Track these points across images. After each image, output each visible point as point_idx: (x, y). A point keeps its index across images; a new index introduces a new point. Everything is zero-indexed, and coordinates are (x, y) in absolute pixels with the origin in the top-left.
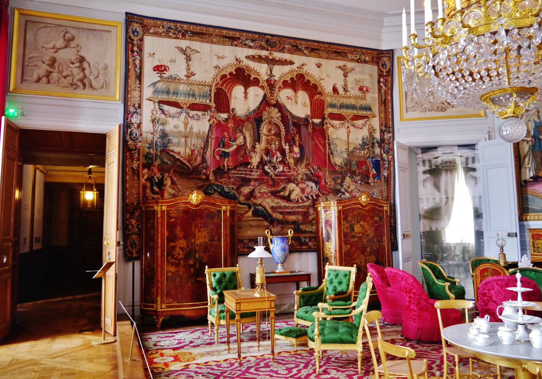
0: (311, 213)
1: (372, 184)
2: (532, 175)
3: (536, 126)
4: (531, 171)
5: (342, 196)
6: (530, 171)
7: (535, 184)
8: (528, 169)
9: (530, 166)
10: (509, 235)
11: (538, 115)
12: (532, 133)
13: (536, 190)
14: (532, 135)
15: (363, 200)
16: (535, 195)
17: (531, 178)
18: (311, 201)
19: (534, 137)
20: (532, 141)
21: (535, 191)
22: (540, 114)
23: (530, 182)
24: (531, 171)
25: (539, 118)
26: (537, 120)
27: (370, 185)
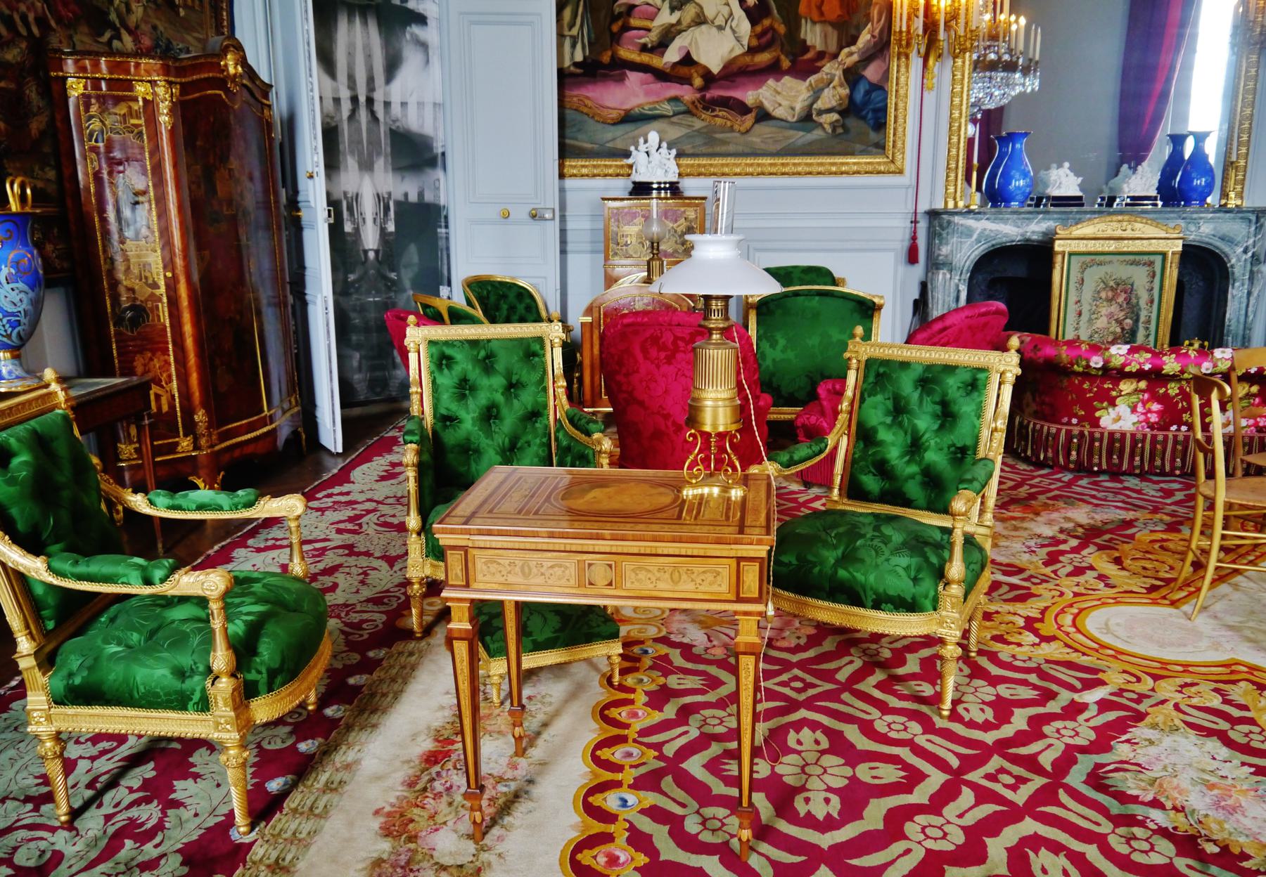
0: (35, 110)
1: (182, 12)
2: (579, 57)
4: (579, 46)
5: (116, 43)
6: (573, 46)
7: (589, 82)
8: (568, 39)
10: (534, 217)
13: (588, 98)
15: (232, 70)
16: (585, 110)
17: (576, 64)
18: (24, 45)
21: (587, 102)
23: (573, 75)
24: (579, 46)
27: (178, 13)
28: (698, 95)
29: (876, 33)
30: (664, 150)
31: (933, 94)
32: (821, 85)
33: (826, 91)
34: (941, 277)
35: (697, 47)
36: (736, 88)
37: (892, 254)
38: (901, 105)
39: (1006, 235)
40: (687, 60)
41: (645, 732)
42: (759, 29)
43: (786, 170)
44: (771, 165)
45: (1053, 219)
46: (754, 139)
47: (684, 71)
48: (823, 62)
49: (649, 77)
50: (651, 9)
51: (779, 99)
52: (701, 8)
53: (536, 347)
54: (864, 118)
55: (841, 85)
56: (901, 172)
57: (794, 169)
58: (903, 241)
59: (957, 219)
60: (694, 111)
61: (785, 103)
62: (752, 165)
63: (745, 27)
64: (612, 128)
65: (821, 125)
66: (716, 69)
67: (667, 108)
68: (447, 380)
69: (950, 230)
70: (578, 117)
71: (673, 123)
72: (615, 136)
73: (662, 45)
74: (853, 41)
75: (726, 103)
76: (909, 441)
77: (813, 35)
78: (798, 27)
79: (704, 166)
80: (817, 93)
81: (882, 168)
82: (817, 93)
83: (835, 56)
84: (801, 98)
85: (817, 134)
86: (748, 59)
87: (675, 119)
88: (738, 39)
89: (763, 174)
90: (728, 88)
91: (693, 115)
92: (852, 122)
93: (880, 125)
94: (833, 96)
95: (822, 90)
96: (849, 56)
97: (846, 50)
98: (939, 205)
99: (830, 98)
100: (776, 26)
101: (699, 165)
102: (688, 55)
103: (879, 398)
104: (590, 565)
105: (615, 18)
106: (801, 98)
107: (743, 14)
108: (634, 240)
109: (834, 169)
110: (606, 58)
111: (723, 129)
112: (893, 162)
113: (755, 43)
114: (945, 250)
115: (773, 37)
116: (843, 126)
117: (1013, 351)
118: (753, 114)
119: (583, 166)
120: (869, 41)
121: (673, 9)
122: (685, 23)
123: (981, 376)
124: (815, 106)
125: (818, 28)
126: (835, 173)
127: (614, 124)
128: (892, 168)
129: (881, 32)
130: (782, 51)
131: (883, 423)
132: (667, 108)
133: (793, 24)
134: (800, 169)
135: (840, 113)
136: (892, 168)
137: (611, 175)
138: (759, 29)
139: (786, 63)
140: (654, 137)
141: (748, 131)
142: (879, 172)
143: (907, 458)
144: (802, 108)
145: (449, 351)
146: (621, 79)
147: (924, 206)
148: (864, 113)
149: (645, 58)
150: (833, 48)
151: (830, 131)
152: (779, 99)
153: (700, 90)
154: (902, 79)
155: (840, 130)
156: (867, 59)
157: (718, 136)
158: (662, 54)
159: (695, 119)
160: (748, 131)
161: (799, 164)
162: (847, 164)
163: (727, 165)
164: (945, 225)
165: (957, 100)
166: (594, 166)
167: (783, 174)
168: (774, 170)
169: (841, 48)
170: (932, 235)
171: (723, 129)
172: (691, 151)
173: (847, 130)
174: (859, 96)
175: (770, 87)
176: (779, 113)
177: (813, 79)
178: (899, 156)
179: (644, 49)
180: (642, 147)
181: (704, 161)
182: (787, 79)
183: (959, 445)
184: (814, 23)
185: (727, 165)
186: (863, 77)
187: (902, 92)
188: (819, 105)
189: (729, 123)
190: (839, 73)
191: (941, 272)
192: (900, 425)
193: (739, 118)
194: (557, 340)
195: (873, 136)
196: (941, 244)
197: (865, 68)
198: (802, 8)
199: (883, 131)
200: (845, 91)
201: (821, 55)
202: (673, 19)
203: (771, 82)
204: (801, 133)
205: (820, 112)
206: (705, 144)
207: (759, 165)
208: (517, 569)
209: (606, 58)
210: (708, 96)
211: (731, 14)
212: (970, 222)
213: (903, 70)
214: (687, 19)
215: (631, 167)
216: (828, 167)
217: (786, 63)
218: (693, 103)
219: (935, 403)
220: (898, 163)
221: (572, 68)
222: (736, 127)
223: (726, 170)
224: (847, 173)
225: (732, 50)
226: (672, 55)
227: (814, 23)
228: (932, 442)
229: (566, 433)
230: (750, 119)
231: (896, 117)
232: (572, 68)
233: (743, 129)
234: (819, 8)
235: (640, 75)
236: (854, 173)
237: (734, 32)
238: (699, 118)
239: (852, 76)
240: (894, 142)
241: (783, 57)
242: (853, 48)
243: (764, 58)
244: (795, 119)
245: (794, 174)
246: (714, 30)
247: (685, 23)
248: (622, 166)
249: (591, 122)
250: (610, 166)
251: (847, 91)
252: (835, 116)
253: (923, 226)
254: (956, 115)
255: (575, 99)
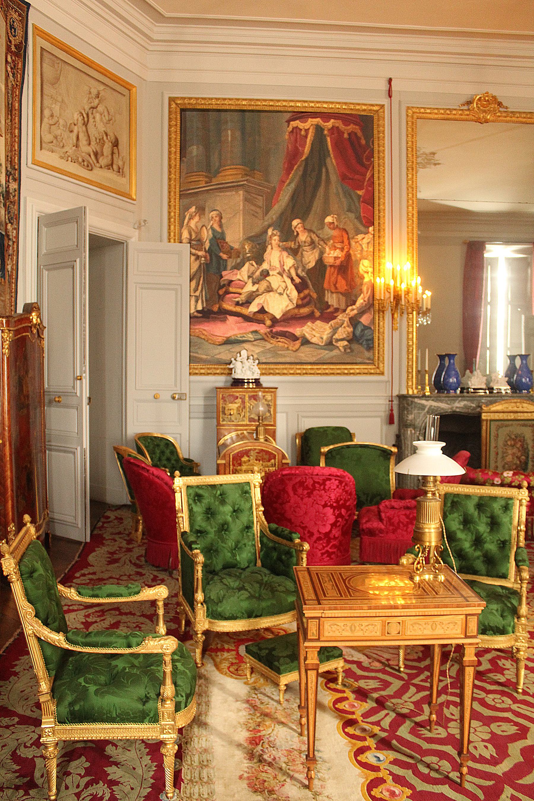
2: (200, 308)
3: (214, 236)
4: (200, 302)
6: (197, 301)
7: (204, 321)
9: (197, 294)
10: (174, 398)
11: (220, 221)
12: (207, 245)
13: (205, 330)
14: (207, 249)
16: (203, 337)
17: (198, 312)
19: (209, 251)
20: (205, 257)
21: (204, 332)
22: (223, 221)
24: (200, 302)
25: (221, 226)
26: (216, 227)
28: (268, 330)
29: (366, 299)
30: (251, 361)
31: (398, 332)
32: (337, 326)
33: (340, 329)
34: (409, 432)
35: (268, 304)
36: (290, 326)
37: (379, 420)
38: (381, 337)
39: (443, 409)
40: (262, 311)
41: (366, 715)
42: (302, 295)
43: (319, 372)
44: (311, 369)
45: (467, 400)
46: (300, 354)
47: (260, 316)
48: (338, 314)
49: (240, 319)
50: (241, 283)
51: (314, 333)
52: (270, 283)
53: (247, 488)
54: (361, 344)
55: (348, 326)
56: (382, 374)
57: (324, 372)
58: (385, 411)
59: (416, 400)
60: (266, 338)
61: (317, 335)
62: (300, 369)
63: (294, 294)
64: (219, 347)
65: (338, 347)
66: (278, 316)
67: (251, 337)
68: (198, 509)
69: (413, 406)
70: (200, 341)
71: (254, 345)
72: (223, 353)
73: (248, 302)
74: (354, 303)
75: (284, 334)
76: (474, 538)
77: (332, 299)
78: (324, 295)
79: (273, 369)
80: (335, 330)
81: (372, 371)
82: (335, 330)
83: (345, 311)
84: (326, 333)
85: (335, 352)
86: (296, 311)
87: (255, 343)
88: (291, 300)
89: (306, 374)
90: (286, 326)
91: (266, 341)
92: (355, 346)
93: (370, 348)
94: (344, 332)
95: (338, 328)
96: (352, 311)
97: (350, 308)
98: (404, 392)
99: (342, 333)
100: (311, 294)
101: (270, 369)
102: (263, 307)
103: (456, 515)
104: (388, 623)
105: (221, 287)
106: (326, 333)
107: (293, 287)
108: (235, 411)
109: (346, 371)
110: (216, 308)
111: (282, 348)
112: (378, 368)
113: (300, 302)
114: (410, 417)
115: (310, 300)
116: (350, 348)
117: (525, 488)
118: (300, 341)
119: (201, 369)
120: (362, 303)
121: (254, 283)
122: (260, 291)
123: (510, 502)
124: (334, 337)
125: (334, 295)
126: (347, 374)
127: (220, 345)
128: (378, 371)
129: (368, 299)
130: (315, 307)
131: (459, 529)
132: (251, 337)
133: (321, 293)
134: (327, 371)
135: (348, 341)
136: (378, 371)
137: (218, 374)
138: (302, 295)
139: (317, 314)
140: (244, 353)
141: (297, 350)
142: (371, 374)
143: (473, 548)
144: (327, 338)
145: (200, 492)
146: (224, 320)
147: (395, 393)
148: (361, 341)
149: (238, 309)
150: (343, 306)
151: (343, 350)
152: (314, 333)
153: (270, 327)
154: (381, 323)
155: (349, 351)
156: (362, 312)
157: (280, 352)
158: (248, 307)
159: (267, 343)
160: (297, 350)
161: (327, 369)
162: (353, 369)
163: (286, 369)
164: (410, 403)
165: (410, 336)
166: (208, 368)
167: (318, 374)
168: (312, 372)
169: (348, 306)
170: (402, 409)
171: (282, 348)
172: (264, 361)
173: (352, 351)
174: (358, 332)
175: (309, 326)
176: (314, 340)
177: (332, 322)
178: (381, 365)
179: (237, 304)
180: (239, 359)
181: (272, 366)
182: (318, 322)
183: (502, 540)
184: (332, 293)
185: (286, 369)
186: (360, 322)
187: (381, 330)
188: (336, 336)
189: (286, 346)
190: (347, 320)
191: (409, 429)
192: (469, 529)
193: (292, 342)
194: (257, 484)
195: (367, 354)
196: (408, 414)
197: (360, 318)
198: (326, 286)
199: (371, 351)
200: (351, 330)
201: (337, 310)
202: (254, 288)
203: (309, 324)
204: (327, 352)
205: (337, 340)
206: (273, 357)
207: (304, 369)
208: (348, 628)
209: (216, 308)
210: (274, 330)
211: (286, 287)
212: (423, 402)
213: (381, 319)
214: (262, 289)
215: (231, 369)
216: (342, 370)
217: (317, 314)
218: (266, 334)
219: (487, 517)
220: (381, 369)
221: (195, 314)
222: (290, 348)
223: (285, 371)
224: (353, 374)
225: (288, 306)
226: (254, 308)
227: (332, 293)
228: (488, 539)
229: (269, 539)
230: (298, 343)
231: (379, 344)
232: (195, 314)
233: (294, 349)
234: (335, 285)
235: (236, 318)
236: (358, 374)
237: (288, 296)
238: (269, 342)
239: (354, 322)
240: (378, 357)
241: (316, 310)
242: (354, 307)
243: (305, 311)
244: (323, 344)
245: (324, 374)
246: (277, 295)
247: (260, 291)
248: (225, 369)
249: (207, 343)
250: (217, 369)
251: (352, 329)
252: (346, 343)
253: (396, 402)
254: (411, 343)
255: (197, 331)
